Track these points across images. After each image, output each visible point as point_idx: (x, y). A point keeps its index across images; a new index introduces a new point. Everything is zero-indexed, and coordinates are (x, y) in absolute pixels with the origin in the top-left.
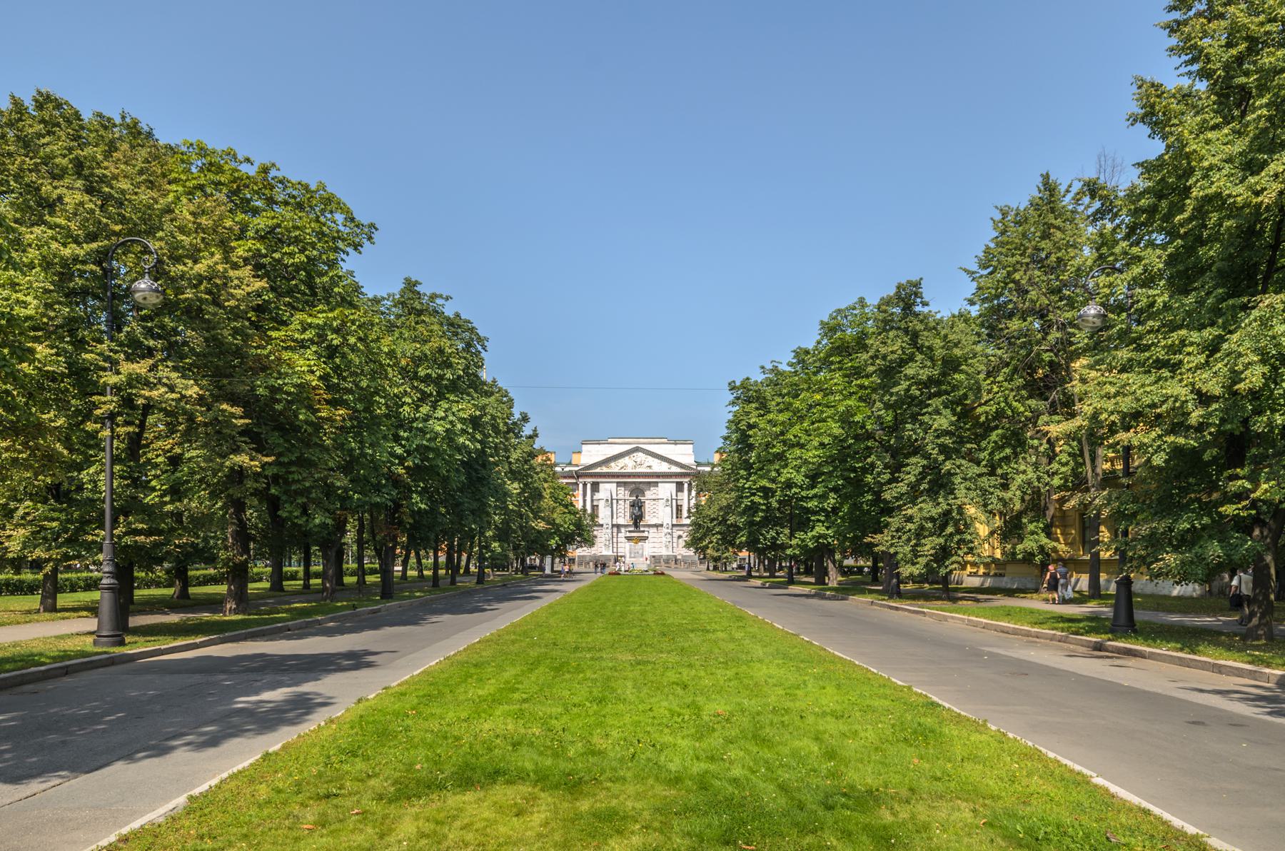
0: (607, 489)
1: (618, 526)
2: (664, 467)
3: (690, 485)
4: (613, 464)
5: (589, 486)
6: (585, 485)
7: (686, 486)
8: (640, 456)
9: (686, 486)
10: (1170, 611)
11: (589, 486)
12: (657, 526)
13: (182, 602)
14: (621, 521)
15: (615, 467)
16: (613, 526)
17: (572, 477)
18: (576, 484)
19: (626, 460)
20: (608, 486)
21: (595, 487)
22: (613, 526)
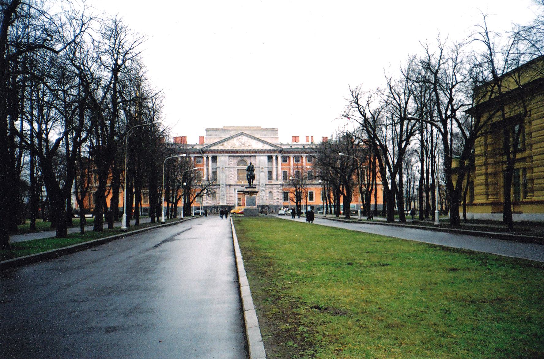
0: (222, 159)
1: (230, 185)
2: (258, 146)
3: (277, 157)
4: (225, 143)
5: (210, 158)
6: (207, 158)
7: (274, 158)
8: (244, 139)
9: (274, 158)
10: (485, 227)
11: (210, 158)
13: (510, 111)
14: (232, 183)
15: (227, 146)
17: (199, 153)
18: (202, 157)
20: (223, 158)
21: (214, 159)
22: (226, 185)
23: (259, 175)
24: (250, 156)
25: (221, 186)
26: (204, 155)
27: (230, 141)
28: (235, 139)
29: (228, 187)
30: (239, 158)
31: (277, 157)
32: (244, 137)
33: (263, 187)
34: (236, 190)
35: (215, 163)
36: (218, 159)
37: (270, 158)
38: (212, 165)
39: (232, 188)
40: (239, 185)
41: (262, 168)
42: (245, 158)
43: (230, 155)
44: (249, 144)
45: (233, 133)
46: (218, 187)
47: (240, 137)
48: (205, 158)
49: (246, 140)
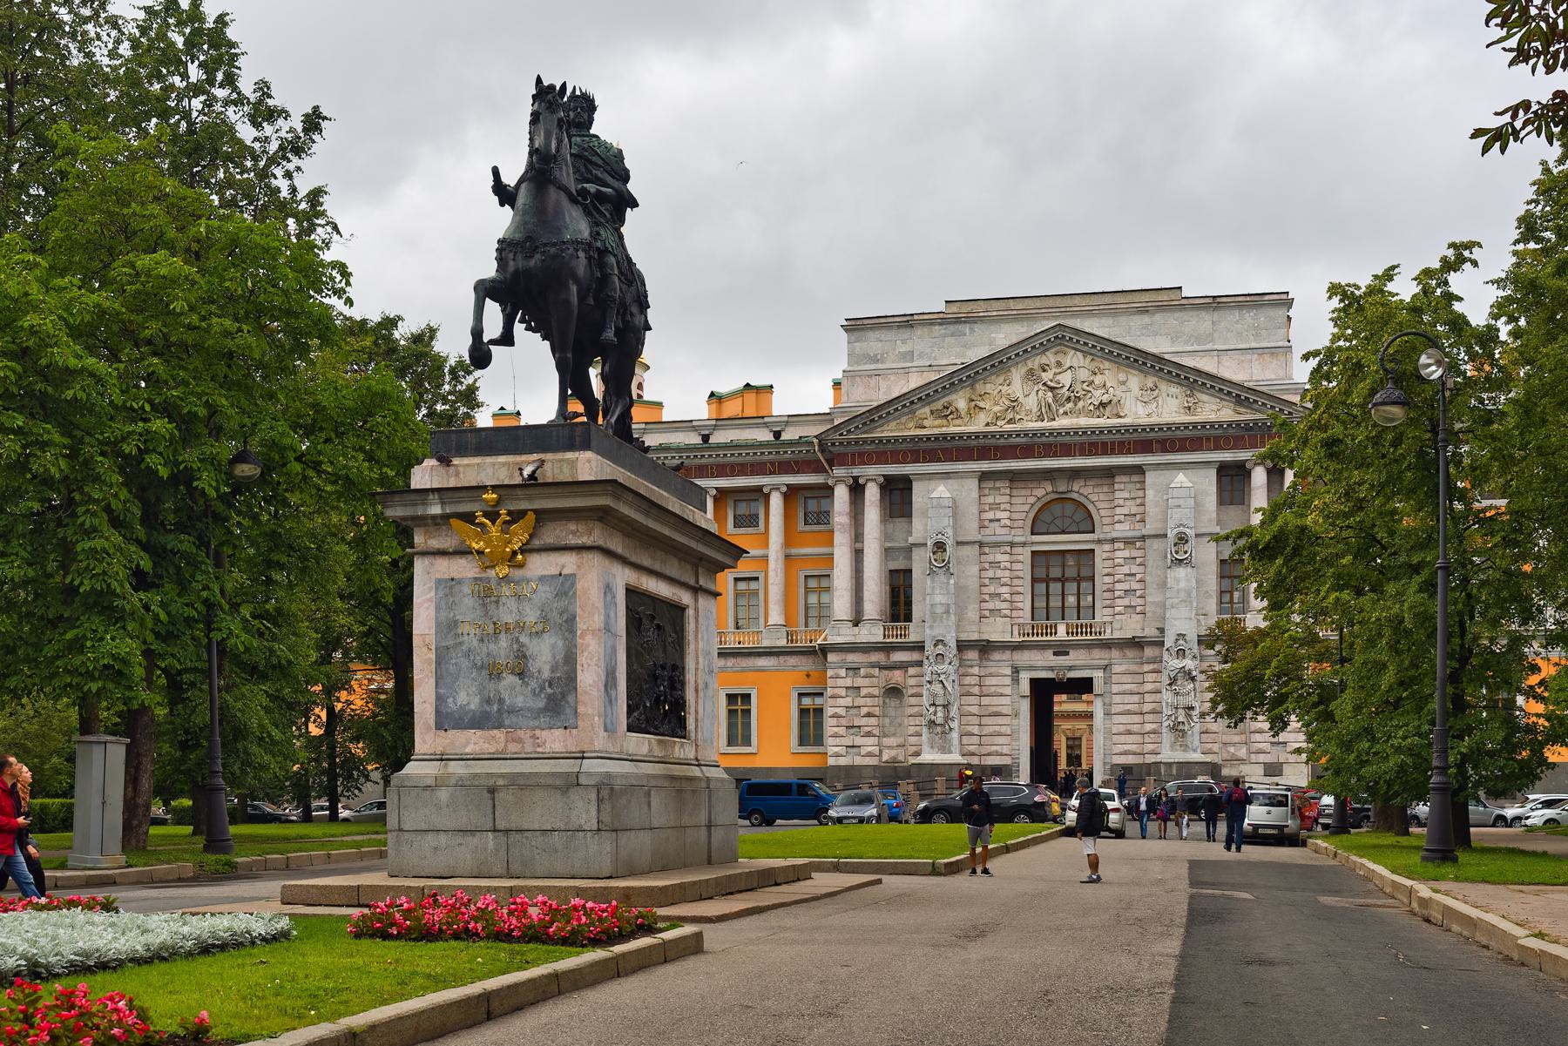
0: (942, 496)
1: (986, 648)
4: (960, 402)
5: (872, 493)
6: (857, 489)
11: (872, 493)
12: (1136, 643)
14: (997, 631)
16: (962, 646)
19: (1016, 384)
20: (941, 490)
22: (962, 646)
23: (1163, 585)
24: (1109, 473)
25: (929, 646)
26: (839, 472)
27: (992, 387)
28: (1017, 375)
29: (972, 655)
30: (1043, 491)
32: (1073, 358)
33: (1181, 653)
34: (1025, 677)
35: (900, 523)
36: (917, 487)
38: (886, 536)
39: (1001, 664)
40: (1042, 647)
41: (1182, 539)
43: (985, 466)
45: (1005, 336)
46: (915, 656)
47: (1050, 358)
48: (841, 494)
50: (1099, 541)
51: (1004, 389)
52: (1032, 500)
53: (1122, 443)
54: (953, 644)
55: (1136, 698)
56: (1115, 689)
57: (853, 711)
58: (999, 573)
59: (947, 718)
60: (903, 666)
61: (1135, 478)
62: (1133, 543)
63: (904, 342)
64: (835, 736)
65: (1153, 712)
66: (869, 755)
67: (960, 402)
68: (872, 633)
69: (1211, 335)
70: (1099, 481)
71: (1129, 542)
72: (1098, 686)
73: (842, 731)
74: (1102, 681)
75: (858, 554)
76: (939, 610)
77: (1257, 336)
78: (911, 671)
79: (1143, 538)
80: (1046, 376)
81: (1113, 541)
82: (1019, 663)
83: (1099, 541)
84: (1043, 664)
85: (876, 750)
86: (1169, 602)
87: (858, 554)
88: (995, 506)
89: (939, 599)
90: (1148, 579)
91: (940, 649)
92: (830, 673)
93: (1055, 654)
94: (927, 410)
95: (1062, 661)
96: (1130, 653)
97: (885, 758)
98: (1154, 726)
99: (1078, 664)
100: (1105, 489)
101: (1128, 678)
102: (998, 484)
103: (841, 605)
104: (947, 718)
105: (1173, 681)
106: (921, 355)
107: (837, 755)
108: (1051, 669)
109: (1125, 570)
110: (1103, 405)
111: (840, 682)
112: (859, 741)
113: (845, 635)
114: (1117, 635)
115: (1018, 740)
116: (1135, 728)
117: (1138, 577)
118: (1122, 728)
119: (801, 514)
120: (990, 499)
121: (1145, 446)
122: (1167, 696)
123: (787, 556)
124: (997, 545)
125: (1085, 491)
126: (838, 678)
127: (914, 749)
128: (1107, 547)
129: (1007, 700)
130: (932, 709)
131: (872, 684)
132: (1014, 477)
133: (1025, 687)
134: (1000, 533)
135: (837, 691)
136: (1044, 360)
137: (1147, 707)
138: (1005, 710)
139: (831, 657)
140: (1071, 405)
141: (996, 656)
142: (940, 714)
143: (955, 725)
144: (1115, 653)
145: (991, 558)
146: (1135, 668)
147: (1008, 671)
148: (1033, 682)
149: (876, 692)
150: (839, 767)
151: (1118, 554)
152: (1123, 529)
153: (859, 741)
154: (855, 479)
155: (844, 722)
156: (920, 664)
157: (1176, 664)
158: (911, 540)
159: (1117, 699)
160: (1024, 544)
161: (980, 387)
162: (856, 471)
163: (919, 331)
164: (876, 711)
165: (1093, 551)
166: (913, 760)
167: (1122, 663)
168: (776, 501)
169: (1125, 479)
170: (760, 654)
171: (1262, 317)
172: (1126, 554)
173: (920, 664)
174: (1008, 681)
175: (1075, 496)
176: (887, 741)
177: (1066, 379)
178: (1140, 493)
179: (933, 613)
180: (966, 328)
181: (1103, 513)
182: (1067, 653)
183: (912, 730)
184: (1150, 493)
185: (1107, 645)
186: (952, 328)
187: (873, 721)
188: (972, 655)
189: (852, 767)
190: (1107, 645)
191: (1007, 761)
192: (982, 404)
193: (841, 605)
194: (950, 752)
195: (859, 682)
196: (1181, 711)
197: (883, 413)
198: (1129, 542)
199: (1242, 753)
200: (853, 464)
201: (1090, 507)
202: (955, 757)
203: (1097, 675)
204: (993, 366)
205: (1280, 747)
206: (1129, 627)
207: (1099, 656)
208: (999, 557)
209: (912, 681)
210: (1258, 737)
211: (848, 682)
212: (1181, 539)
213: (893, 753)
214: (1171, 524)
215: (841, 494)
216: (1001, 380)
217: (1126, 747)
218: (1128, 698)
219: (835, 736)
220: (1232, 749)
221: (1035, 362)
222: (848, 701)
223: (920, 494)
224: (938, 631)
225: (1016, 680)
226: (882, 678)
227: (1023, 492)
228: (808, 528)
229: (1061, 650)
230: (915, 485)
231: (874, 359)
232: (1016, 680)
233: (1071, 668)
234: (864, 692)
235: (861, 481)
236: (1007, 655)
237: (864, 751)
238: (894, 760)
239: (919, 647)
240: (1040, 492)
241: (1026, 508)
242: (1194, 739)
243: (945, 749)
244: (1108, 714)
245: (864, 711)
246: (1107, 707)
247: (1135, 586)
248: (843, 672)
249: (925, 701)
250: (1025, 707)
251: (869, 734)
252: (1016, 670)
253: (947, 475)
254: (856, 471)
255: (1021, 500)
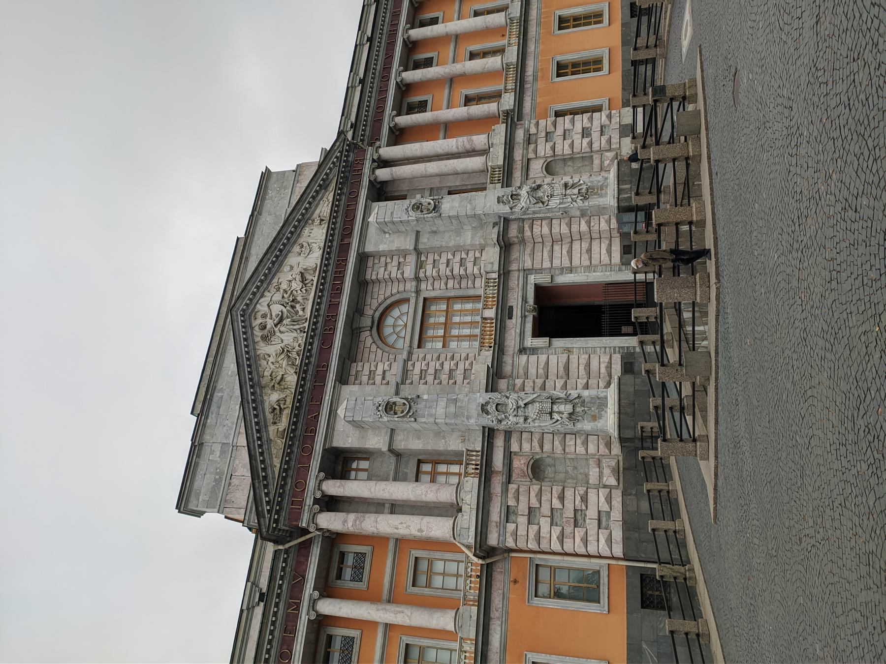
3: (385, 163)
5: (333, 487)
7: (383, 174)
8: (270, 305)
9: (383, 174)
11: (333, 487)
12: (505, 246)
21: (339, 463)
25: (489, 421)
27: (267, 368)
28: (264, 349)
31: (385, 163)
34: (530, 342)
37: (382, 192)
39: (513, 362)
42: (369, 311)
44: (296, 285)
46: (499, 442)
47: (256, 323)
48: (330, 521)
49: (278, 297)
50: (418, 292)
51: (271, 359)
52: (374, 347)
53: (338, 266)
54: (490, 395)
55: (557, 248)
56: (547, 264)
57: (557, 515)
58: (431, 371)
59: (567, 400)
60: (509, 456)
61: (370, 264)
62: (422, 262)
63: (212, 452)
64: (585, 541)
65: (569, 225)
66: (609, 499)
67: (272, 398)
68: (472, 484)
69: (276, 216)
70: (369, 295)
71: (420, 265)
72: (544, 279)
73: (579, 533)
74: (539, 276)
75: (395, 507)
76: (452, 409)
77: (285, 188)
78: (515, 447)
79: (418, 253)
80: (270, 323)
81: (418, 279)
82: (517, 348)
83: (418, 292)
84: (519, 328)
85: (603, 493)
86: (469, 212)
87: (395, 507)
88: (372, 374)
89: (440, 410)
90: (451, 244)
91: (491, 408)
92: (510, 543)
93: (510, 318)
94: (272, 429)
95: (517, 312)
96: (515, 254)
97: (612, 481)
98: (583, 222)
99: (521, 298)
100: (376, 289)
101: (538, 255)
102: (353, 372)
103: (438, 528)
104: (567, 400)
105: (540, 200)
106: (227, 437)
107: (609, 541)
108: (524, 317)
109: (443, 267)
110: (303, 280)
111: (522, 531)
112: (592, 513)
113: (468, 519)
114: (496, 268)
115: (594, 348)
116: (585, 245)
117: (450, 256)
118: (585, 256)
119: (352, 585)
120: (365, 379)
121: (344, 249)
122: (554, 203)
123: (389, 602)
124: (405, 372)
125: (375, 304)
126: (518, 534)
127: (603, 450)
128: (423, 286)
129: (553, 359)
130: (556, 416)
131: (526, 494)
132: (350, 355)
133: (542, 342)
134: (397, 368)
135: (532, 535)
136: (257, 328)
137: (565, 229)
138: (563, 358)
139: (493, 540)
140: (298, 306)
141: (507, 369)
142: (562, 408)
143: (574, 394)
144: (514, 267)
145: (416, 378)
146: (528, 250)
147: (524, 358)
148: (536, 334)
149: (535, 488)
150: (626, 540)
151: (428, 273)
152: (409, 271)
153: (592, 513)
154: (316, 501)
155: (569, 530)
156: (508, 434)
157: (523, 202)
158: (385, 449)
159: (557, 263)
160: (410, 353)
161: (263, 382)
162: (309, 501)
163: (207, 437)
164: (557, 490)
165: (425, 299)
166: (616, 449)
167: (522, 259)
168: (328, 607)
169: (369, 271)
170: (486, 643)
171: (273, 184)
172: (429, 267)
173: (508, 434)
174: (533, 358)
175: (377, 314)
176: (593, 480)
177: (277, 309)
178: (383, 259)
179: (455, 416)
180: (217, 395)
181: (395, 291)
182: (511, 308)
183: (580, 449)
184: (382, 247)
185: (504, 273)
186: (214, 407)
187: (569, 493)
188: (503, 384)
189: (625, 522)
190: (504, 273)
191: (617, 358)
192: (279, 378)
193: (438, 528)
194: (606, 398)
195: (523, 508)
196: (568, 192)
197: (260, 466)
198: (420, 265)
199: (610, 155)
200: (301, 503)
201: (388, 302)
202: (612, 394)
203: (532, 279)
204: (249, 366)
205: (606, 130)
206: (492, 255)
207: (515, 281)
208: (417, 371)
209: (526, 447)
210: (596, 146)
211: (522, 520)
212: (418, 208)
213: (607, 472)
214: (405, 217)
215: (330, 521)
216: (264, 363)
217: (604, 251)
218: (557, 254)
219: (585, 541)
220: (607, 163)
221: (258, 333)
222: (545, 523)
223: (346, 438)
224: (474, 409)
225: (534, 351)
226: (521, 482)
227: (366, 355)
228: (365, 578)
229: (505, 312)
230: (335, 444)
231: (217, 482)
232: (534, 351)
233: (525, 300)
234: (534, 503)
235: (318, 496)
236: (508, 359)
237: (605, 507)
238: (616, 471)
239: (489, 434)
240: (369, 341)
241: (380, 352)
242: (598, 179)
243: (602, 403)
244: (571, 270)
245: (556, 504)
246: (562, 270)
247: (458, 259)
248: (511, 527)
249: (546, 423)
250: (559, 343)
251: (585, 499)
252: (522, 350)
253: (333, 413)
254: (309, 501)
255: (372, 356)
